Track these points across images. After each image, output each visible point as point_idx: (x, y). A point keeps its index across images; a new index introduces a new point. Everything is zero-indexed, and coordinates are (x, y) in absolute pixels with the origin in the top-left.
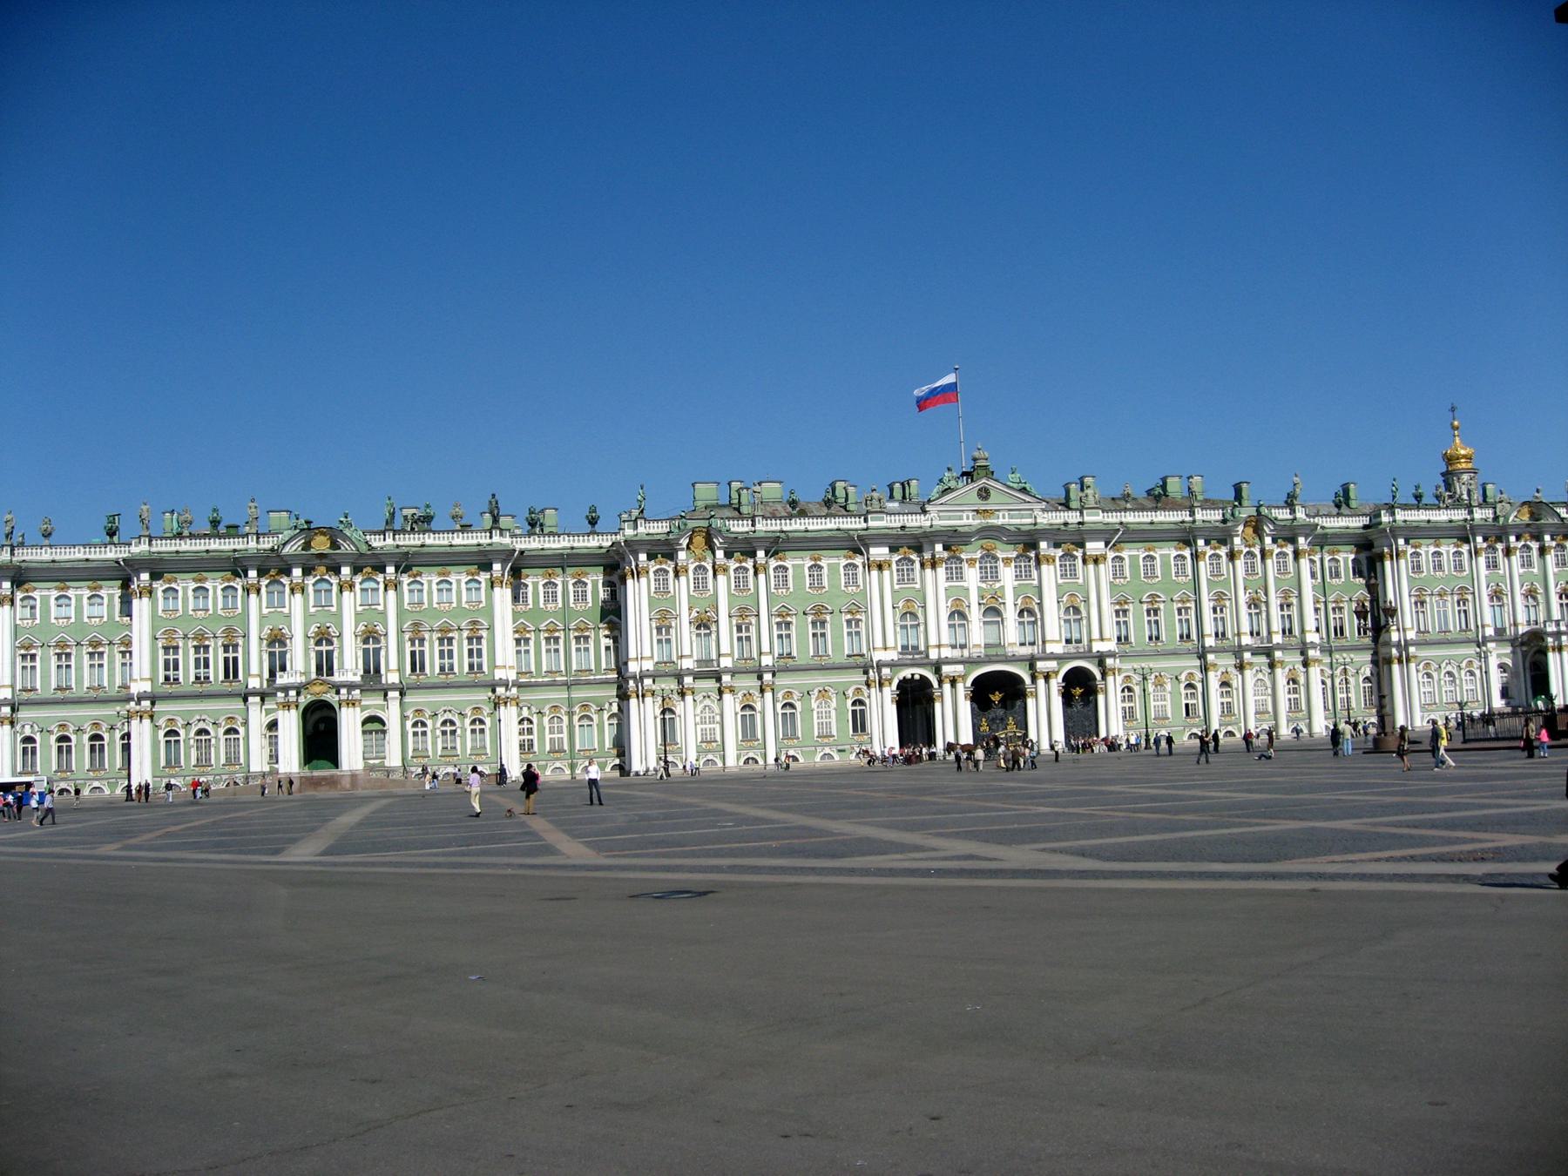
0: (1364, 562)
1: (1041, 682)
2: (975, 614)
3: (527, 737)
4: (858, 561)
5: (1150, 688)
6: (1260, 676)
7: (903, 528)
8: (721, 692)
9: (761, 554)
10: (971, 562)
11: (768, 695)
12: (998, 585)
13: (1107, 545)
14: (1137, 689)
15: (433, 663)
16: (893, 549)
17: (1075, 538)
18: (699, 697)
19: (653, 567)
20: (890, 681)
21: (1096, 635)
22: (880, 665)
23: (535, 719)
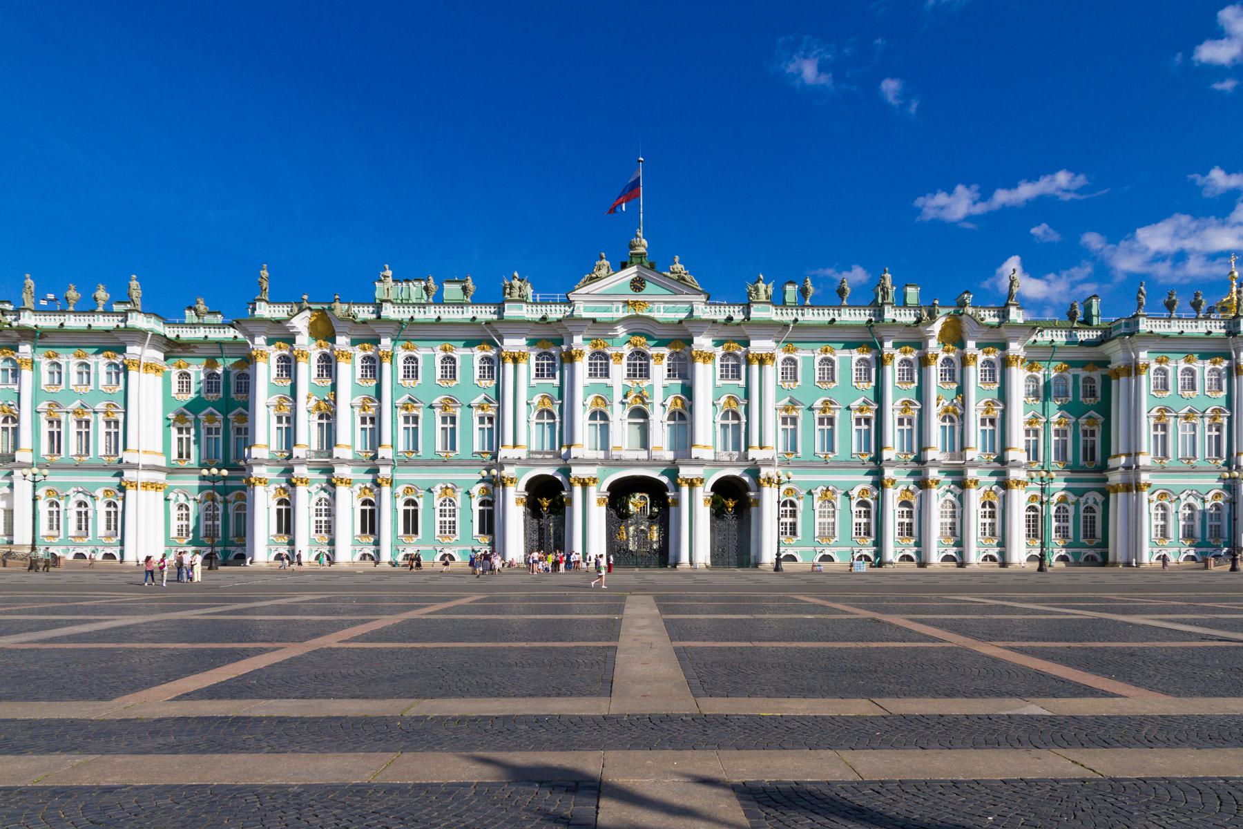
1: (685, 490)
5: (817, 504)
7: (544, 318)
9: (386, 343)
11: (386, 490)
12: (645, 383)
14: (800, 505)
15: (71, 445)
16: (532, 343)
21: (755, 441)
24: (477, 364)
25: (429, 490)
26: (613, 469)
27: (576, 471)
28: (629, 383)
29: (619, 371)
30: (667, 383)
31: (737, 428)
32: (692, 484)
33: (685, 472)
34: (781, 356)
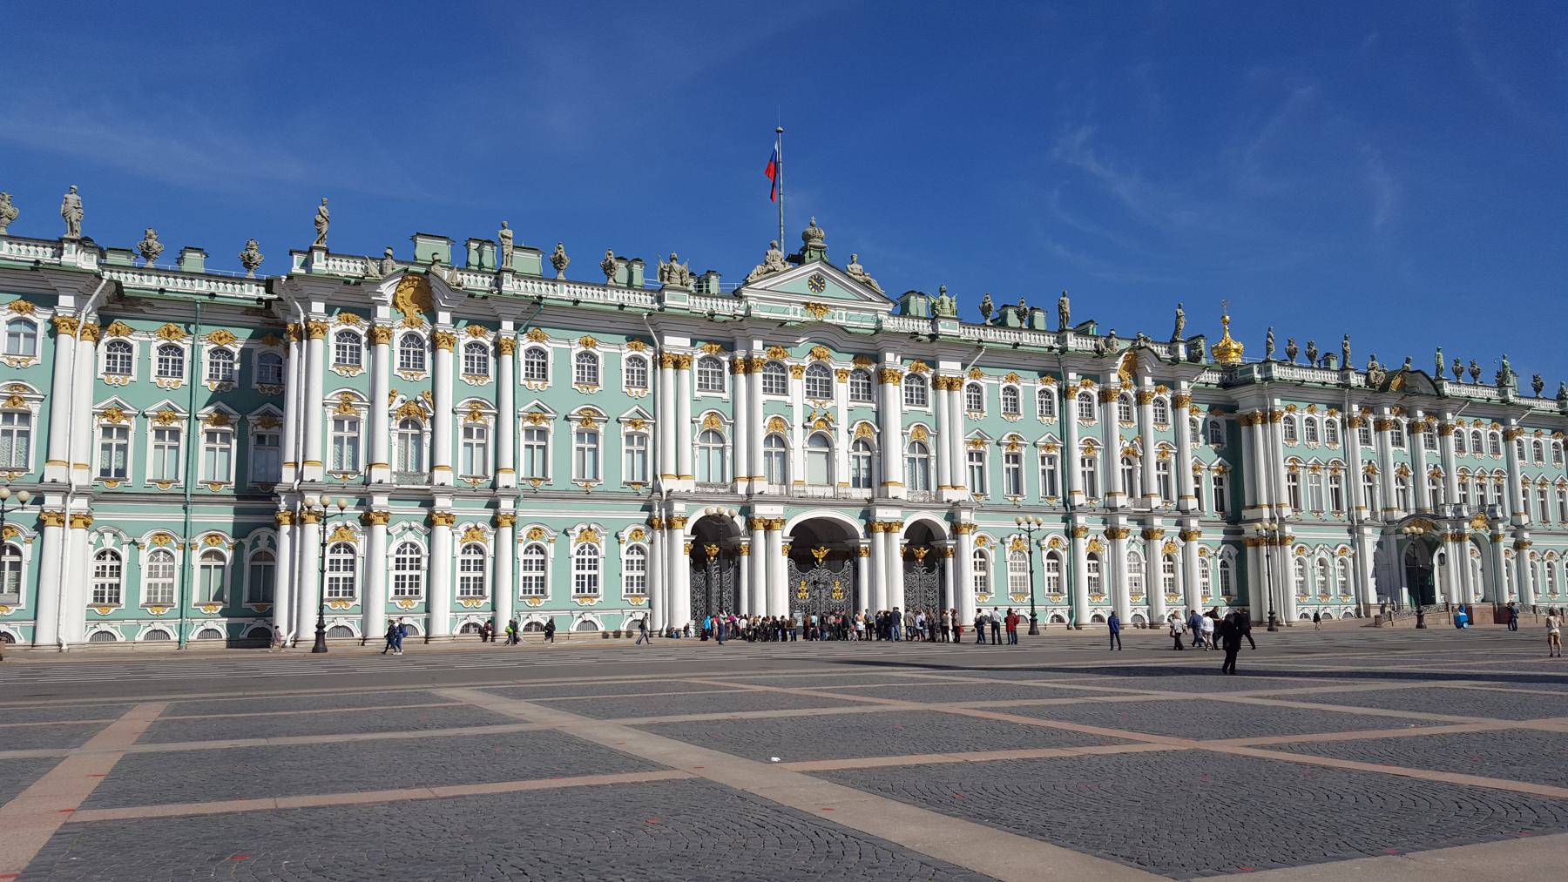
0: (1223, 427)
1: (881, 536)
2: (798, 440)
3: (108, 580)
4: (647, 354)
5: (1008, 556)
6: (1134, 548)
7: (712, 315)
8: (430, 523)
9: (507, 326)
10: (798, 370)
11: (506, 532)
12: (829, 405)
13: (964, 366)
17: (927, 350)
18: (396, 529)
19: (335, 326)
20: (684, 520)
22: (671, 498)
23: (125, 553)
24: (624, 366)
25: (565, 532)
26: (796, 509)
27: (761, 511)
28: (811, 403)
29: (797, 386)
30: (852, 404)
31: (925, 462)
32: (888, 529)
33: (882, 514)
34: (968, 381)
